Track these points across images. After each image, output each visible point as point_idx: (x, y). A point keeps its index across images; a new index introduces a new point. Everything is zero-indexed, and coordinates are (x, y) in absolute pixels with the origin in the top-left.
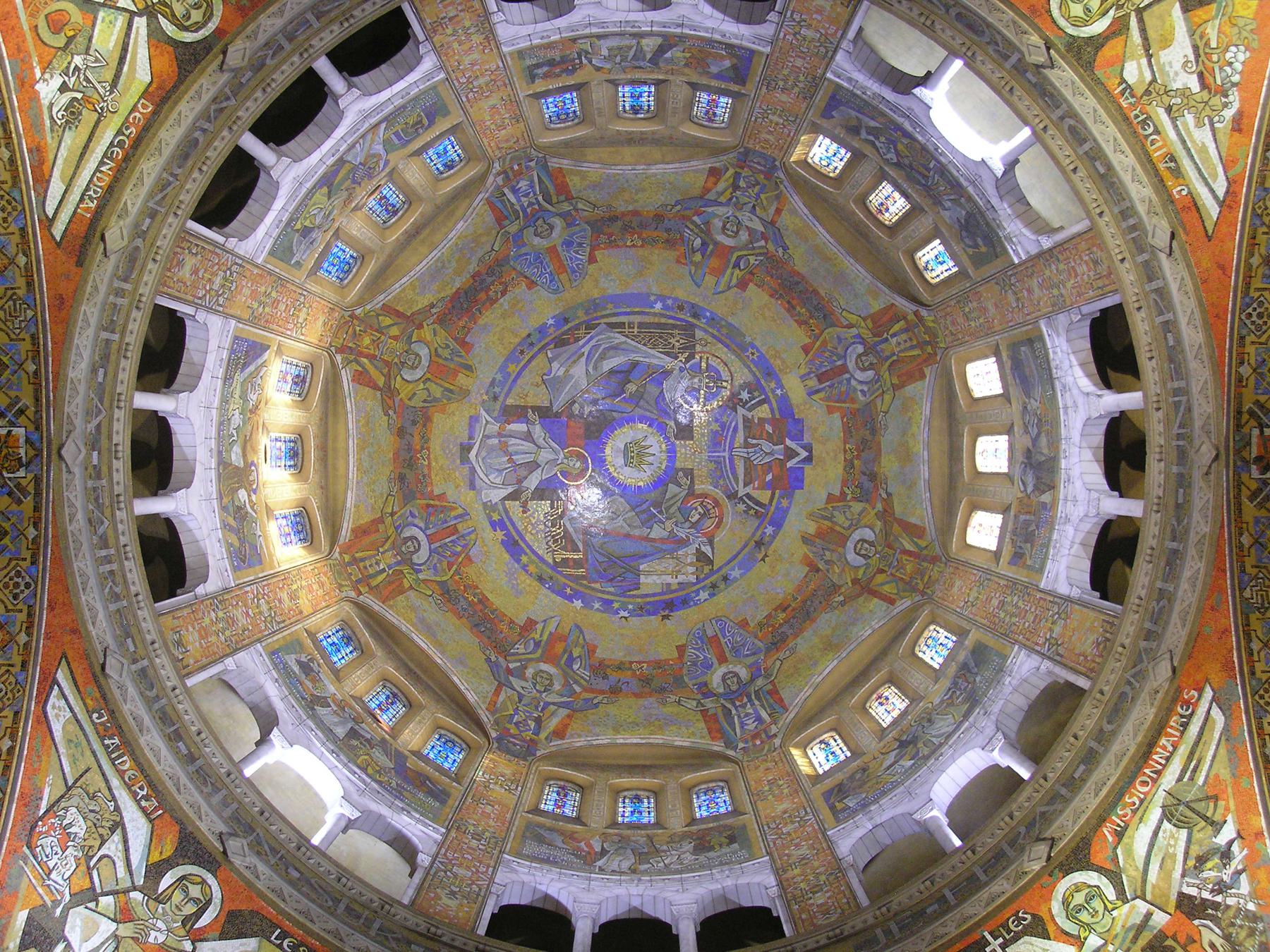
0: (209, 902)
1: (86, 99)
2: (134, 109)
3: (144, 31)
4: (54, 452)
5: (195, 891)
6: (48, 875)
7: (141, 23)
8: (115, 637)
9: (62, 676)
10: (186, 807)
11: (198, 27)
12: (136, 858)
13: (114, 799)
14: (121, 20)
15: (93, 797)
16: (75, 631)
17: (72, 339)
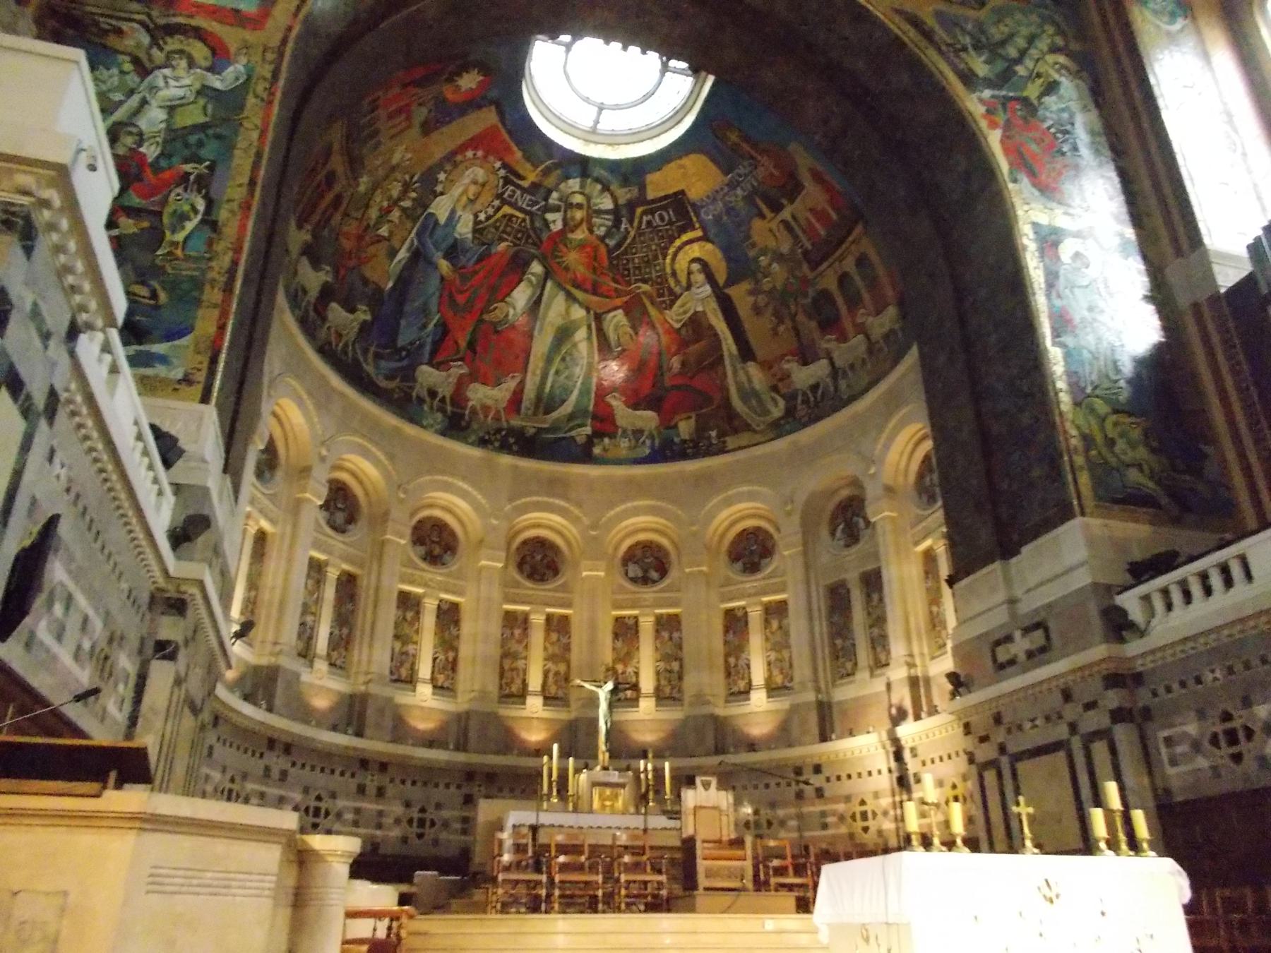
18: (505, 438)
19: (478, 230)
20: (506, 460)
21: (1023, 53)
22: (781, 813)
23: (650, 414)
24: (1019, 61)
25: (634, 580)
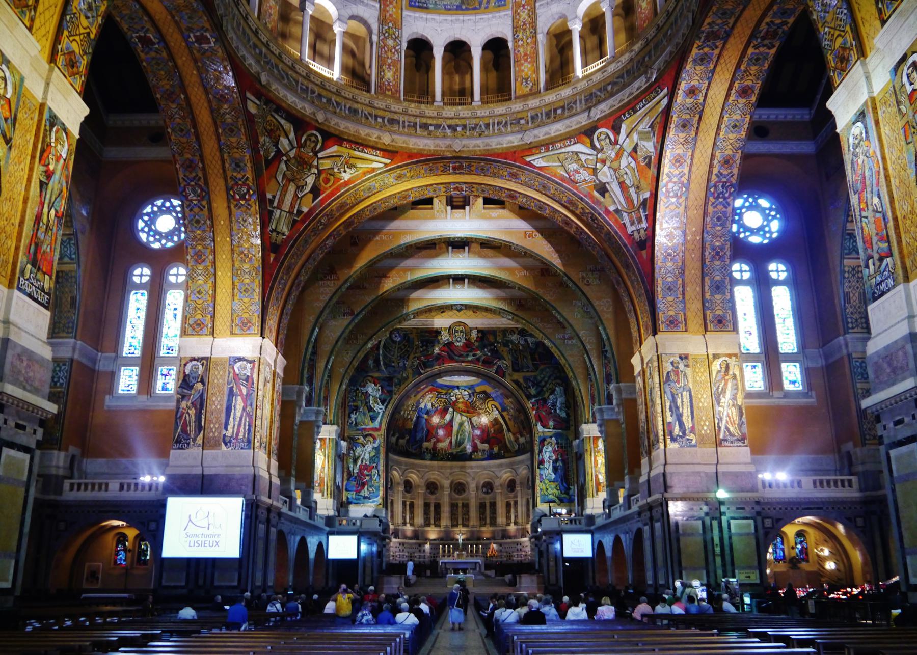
0: (607, 134)
1: (347, 163)
2: (346, 147)
3: (322, 153)
4: (457, 155)
5: (603, 137)
6: (585, 180)
7: (320, 155)
8: (518, 132)
9: (528, 159)
10: (576, 127)
11: (316, 137)
12: (589, 152)
13: (568, 152)
14: (321, 161)
15: (567, 159)
16: (515, 152)
17: (421, 149)
18: (448, 457)
19: (433, 405)
20: (449, 463)
21: (546, 383)
22: (514, 554)
23: (487, 445)
24: (545, 386)
25: (484, 493)
